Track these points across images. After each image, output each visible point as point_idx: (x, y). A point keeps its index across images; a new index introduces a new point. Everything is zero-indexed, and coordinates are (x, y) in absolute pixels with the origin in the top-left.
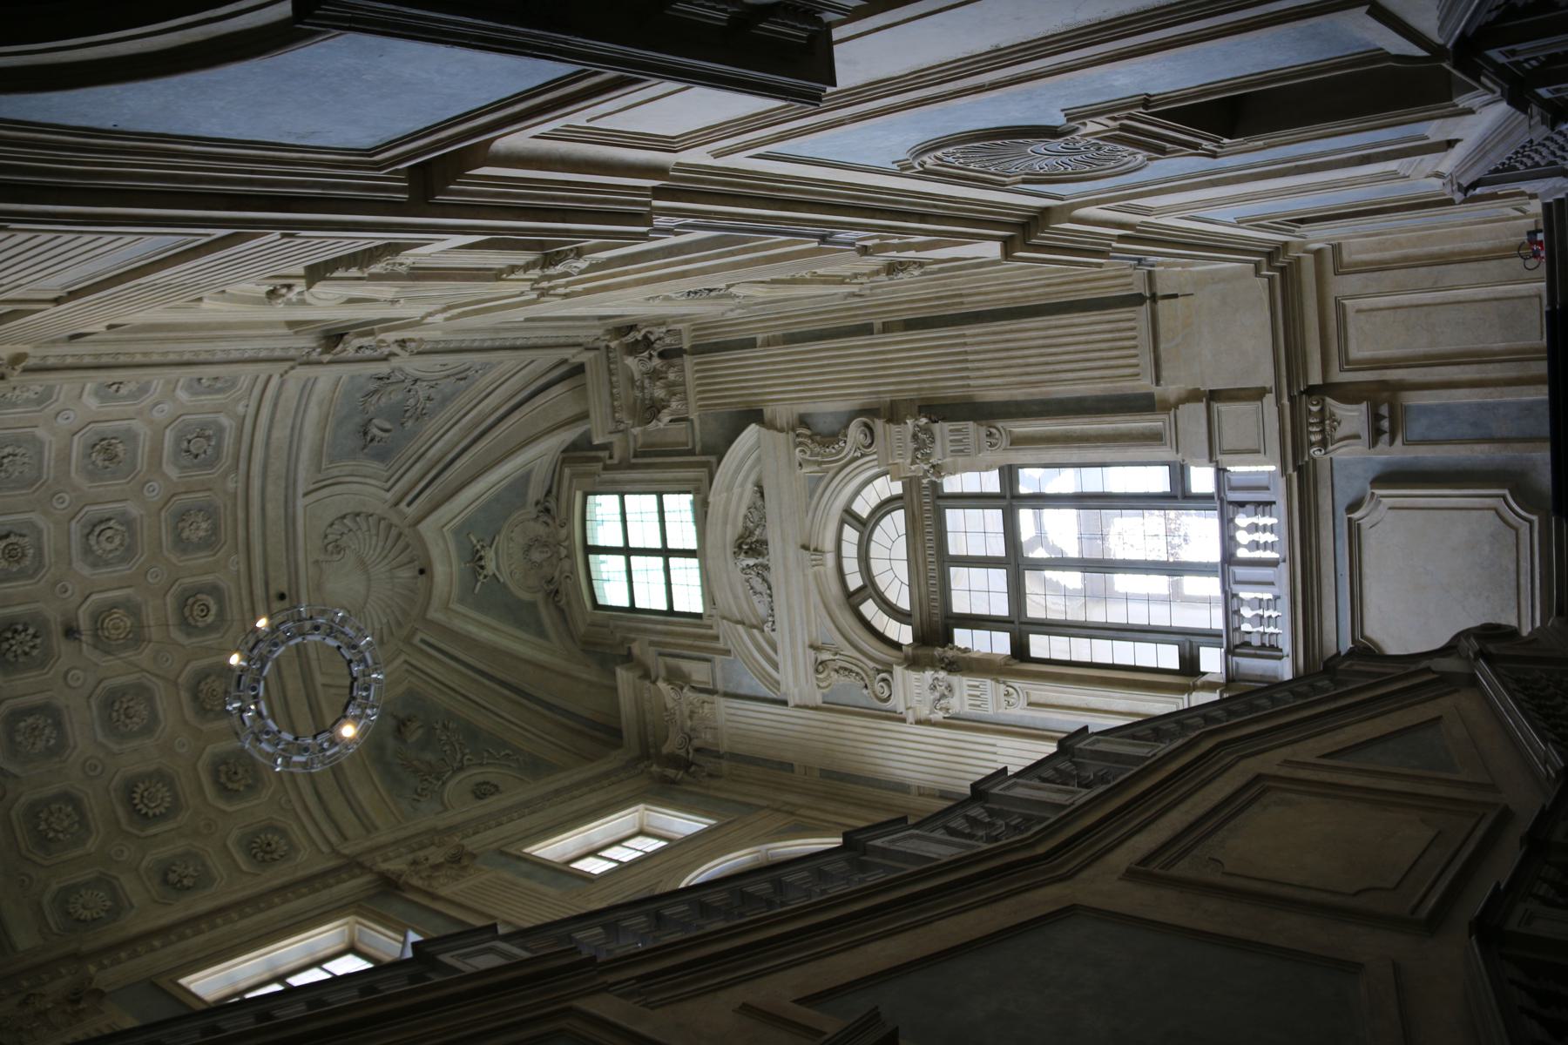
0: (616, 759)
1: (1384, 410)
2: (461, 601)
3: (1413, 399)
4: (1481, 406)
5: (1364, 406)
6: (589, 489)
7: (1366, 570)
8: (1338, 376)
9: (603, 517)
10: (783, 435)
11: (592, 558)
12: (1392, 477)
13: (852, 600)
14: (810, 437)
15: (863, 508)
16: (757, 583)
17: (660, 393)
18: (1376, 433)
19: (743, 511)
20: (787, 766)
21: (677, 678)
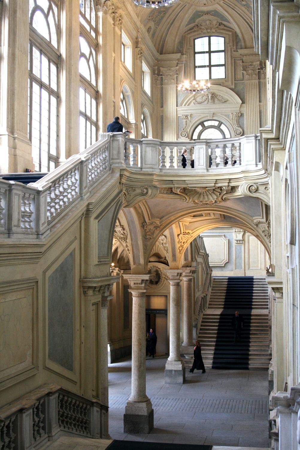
0: (157, 55)
1: (241, 242)
2: (196, 11)
4: (241, 258)
5: (242, 239)
6: (226, 39)
7: (214, 238)
9: (218, 43)
10: (239, 109)
11: (207, 38)
12: (229, 242)
13: (202, 124)
14: (239, 116)
15: (223, 127)
16: (204, 98)
17: (250, 71)
18: (237, 241)
19: (221, 95)
20: (162, 107)
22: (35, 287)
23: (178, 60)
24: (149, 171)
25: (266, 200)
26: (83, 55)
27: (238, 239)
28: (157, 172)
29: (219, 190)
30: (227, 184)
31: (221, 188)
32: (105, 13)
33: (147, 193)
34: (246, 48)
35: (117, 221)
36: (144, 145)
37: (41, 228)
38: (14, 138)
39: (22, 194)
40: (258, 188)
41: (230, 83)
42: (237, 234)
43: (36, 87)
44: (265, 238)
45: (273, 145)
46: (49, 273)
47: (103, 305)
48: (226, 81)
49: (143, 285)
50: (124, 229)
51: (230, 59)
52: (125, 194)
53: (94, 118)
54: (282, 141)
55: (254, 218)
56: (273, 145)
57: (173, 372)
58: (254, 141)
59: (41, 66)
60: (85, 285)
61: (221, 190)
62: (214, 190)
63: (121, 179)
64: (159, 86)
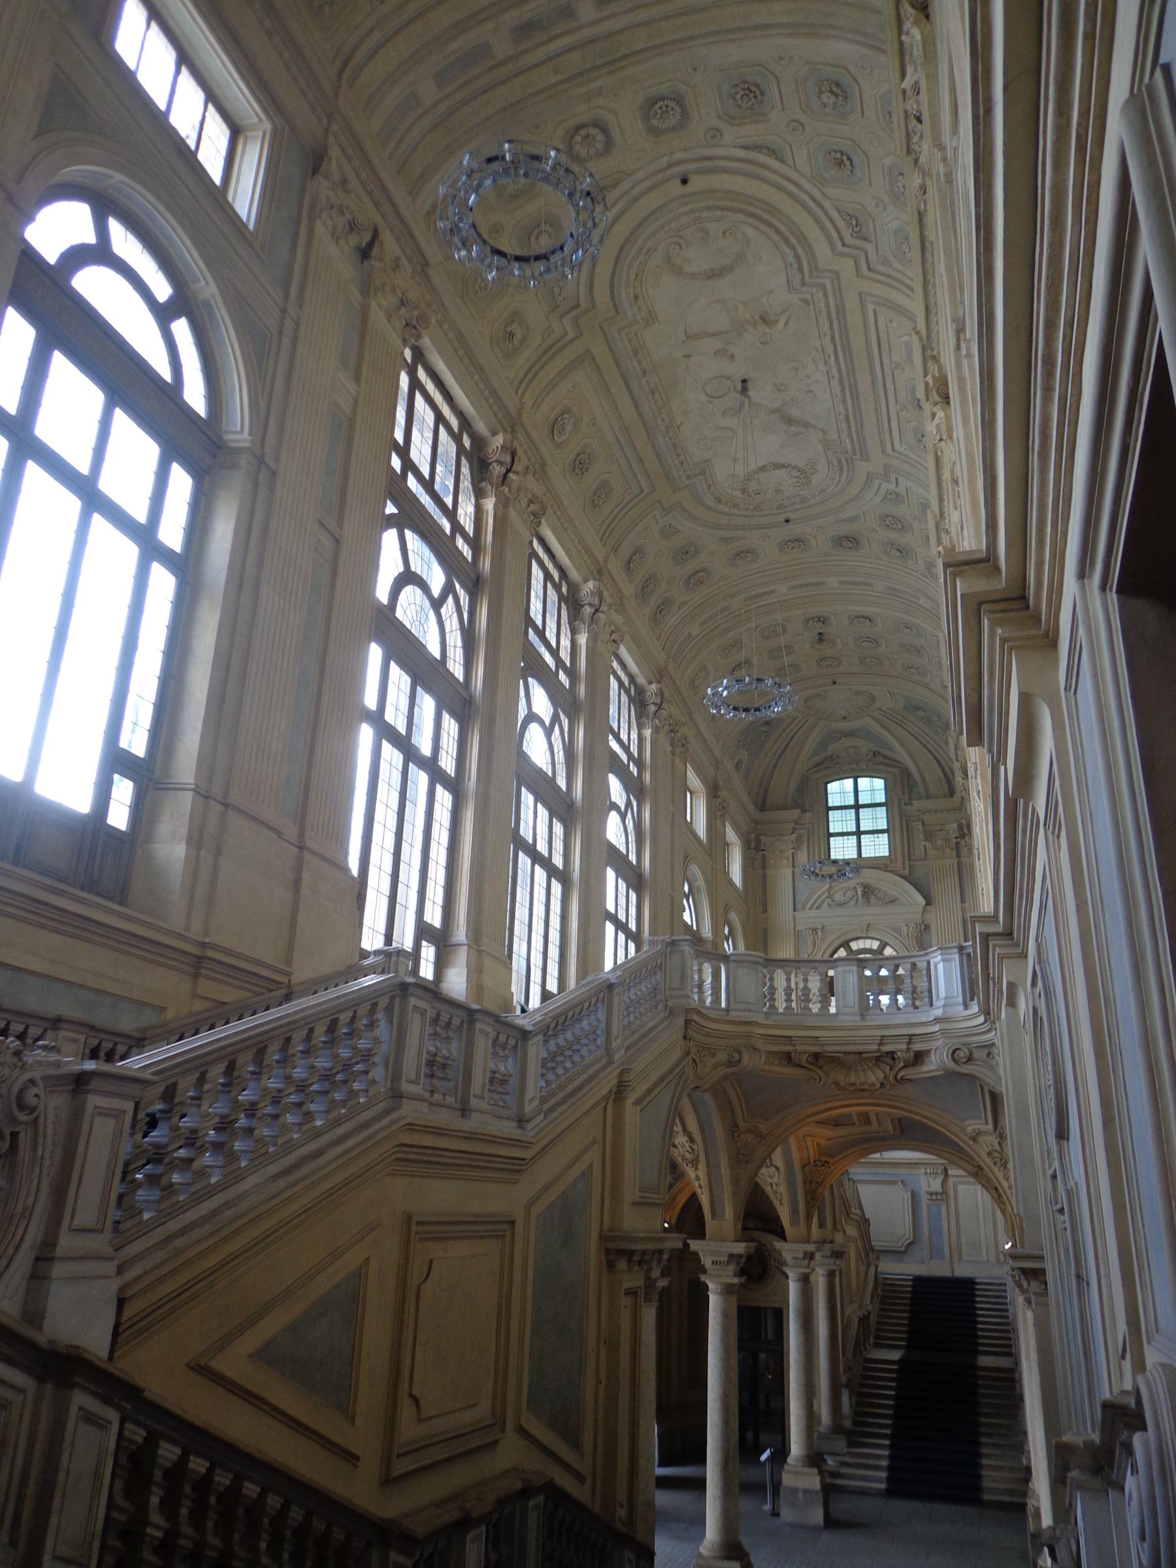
3: (944, 1208)
8: (951, 1181)
16: (849, 894)
17: (939, 842)
18: (931, 1194)
20: (765, 911)
21: (799, 841)
22: (508, 1234)
23: (796, 822)
24: (745, 1016)
25: (990, 1081)
26: (614, 806)
27: (931, 1190)
28: (760, 1019)
29: (889, 1060)
30: (904, 1046)
31: (892, 1055)
32: (656, 731)
33: (740, 1061)
34: (928, 797)
35: (677, 1120)
36: (732, 965)
37: (527, 1109)
38: (480, 952)
39: (492, 1035)
40: (971, 1053)
41: (900, 864)
42: (931, 1181)
43: (524, 861)
44: (995, 1169)
45: (997, 949)
46: (537, 1210)
47: (647, 1298)
48: (891, 862)
49: (732, 1267)
50: (692, 1140)
51: (897, 820)
52: (694, 1061)
53: (633, 926)
54: (1019, 937)
55: (967, 1123)
56: (997, 949)
57: (801, 1496)
58: (957, 956)
59: (535, 820)
60: (610, 1245)
61: (893, 1059)
62: (878, 1059)
63: (686, 1028)
64: (760, 872)
